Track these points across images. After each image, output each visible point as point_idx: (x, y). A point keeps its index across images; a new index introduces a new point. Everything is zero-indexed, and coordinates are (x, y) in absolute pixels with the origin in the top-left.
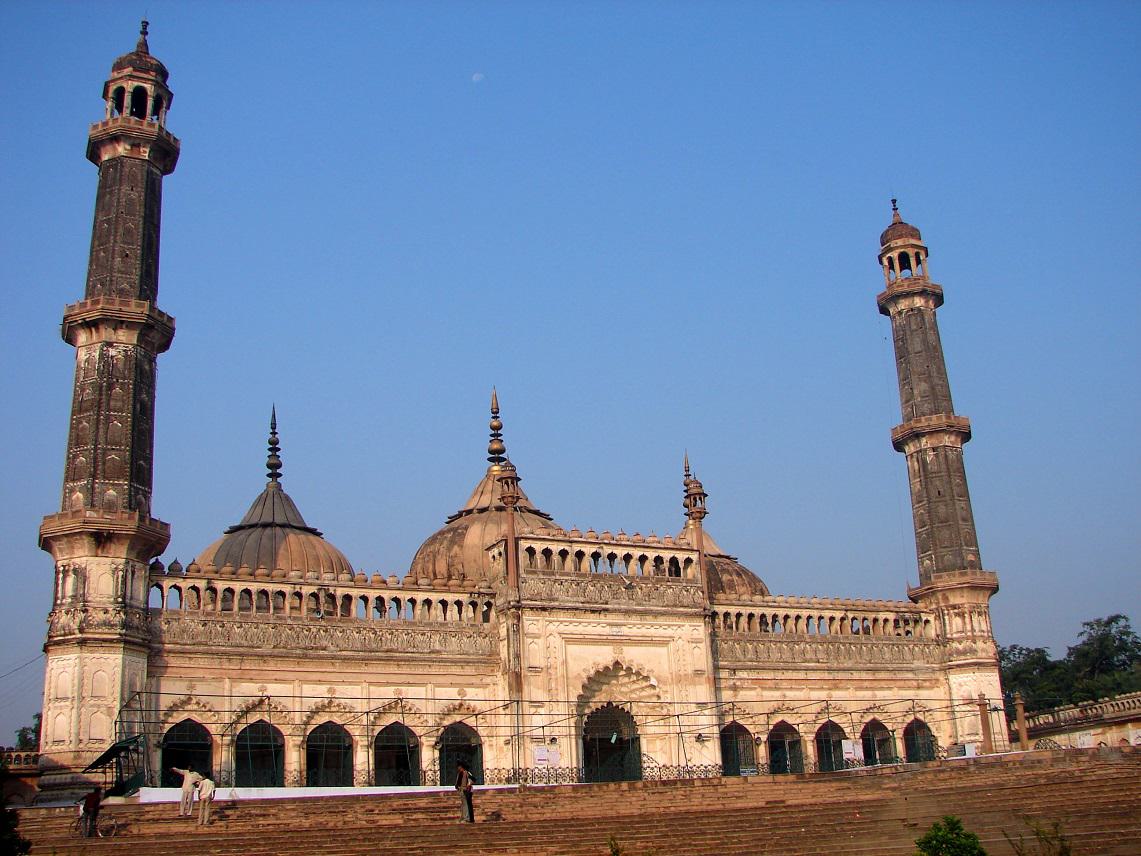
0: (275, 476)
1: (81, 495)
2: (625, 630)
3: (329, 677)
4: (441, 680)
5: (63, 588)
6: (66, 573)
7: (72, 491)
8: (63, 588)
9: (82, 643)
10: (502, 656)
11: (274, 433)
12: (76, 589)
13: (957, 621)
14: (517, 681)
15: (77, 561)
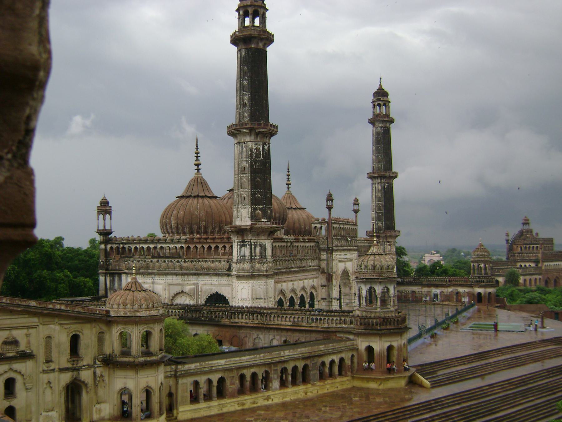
0: (198, 170)
1: (260, 212)
2: (347, 256)
3: (293, 279)
4: (310, 277)
5: (255, 252)
6: (255, 246)
7: (255, 209)
8: (255, 252)
9: (268, 276)
10: (322, 267)
11: (197, 149)
12: (261, 253)
13: (389, 247)
14: (329, 278)
15: (262, 241)
